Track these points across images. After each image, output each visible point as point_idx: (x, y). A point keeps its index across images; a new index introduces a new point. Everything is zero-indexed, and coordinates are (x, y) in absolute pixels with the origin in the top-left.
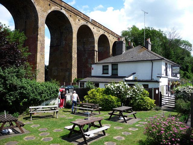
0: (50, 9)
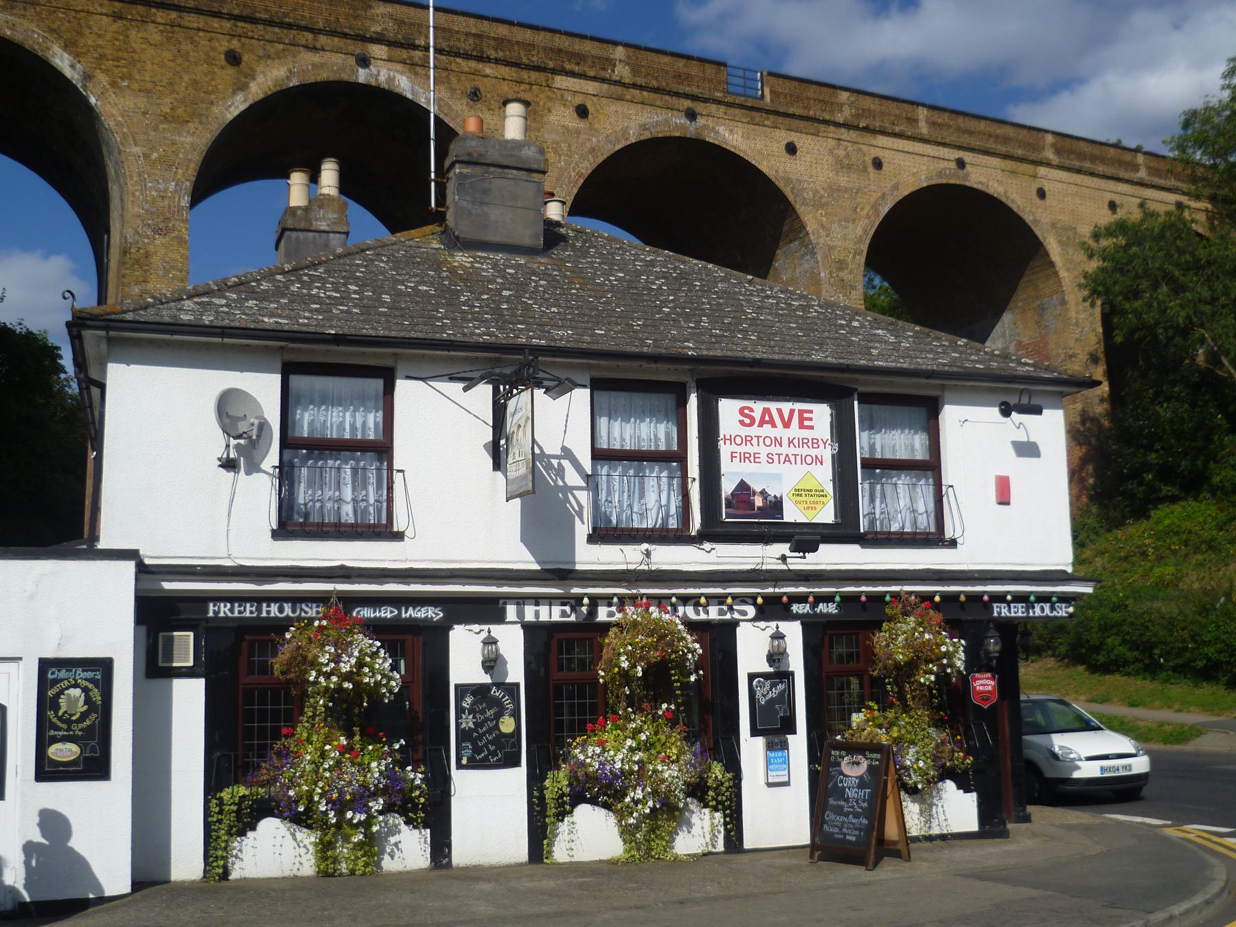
0: (243, 87)
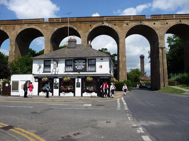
0: (91, 28)
